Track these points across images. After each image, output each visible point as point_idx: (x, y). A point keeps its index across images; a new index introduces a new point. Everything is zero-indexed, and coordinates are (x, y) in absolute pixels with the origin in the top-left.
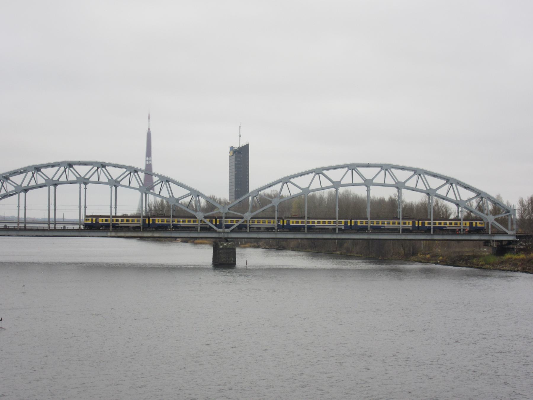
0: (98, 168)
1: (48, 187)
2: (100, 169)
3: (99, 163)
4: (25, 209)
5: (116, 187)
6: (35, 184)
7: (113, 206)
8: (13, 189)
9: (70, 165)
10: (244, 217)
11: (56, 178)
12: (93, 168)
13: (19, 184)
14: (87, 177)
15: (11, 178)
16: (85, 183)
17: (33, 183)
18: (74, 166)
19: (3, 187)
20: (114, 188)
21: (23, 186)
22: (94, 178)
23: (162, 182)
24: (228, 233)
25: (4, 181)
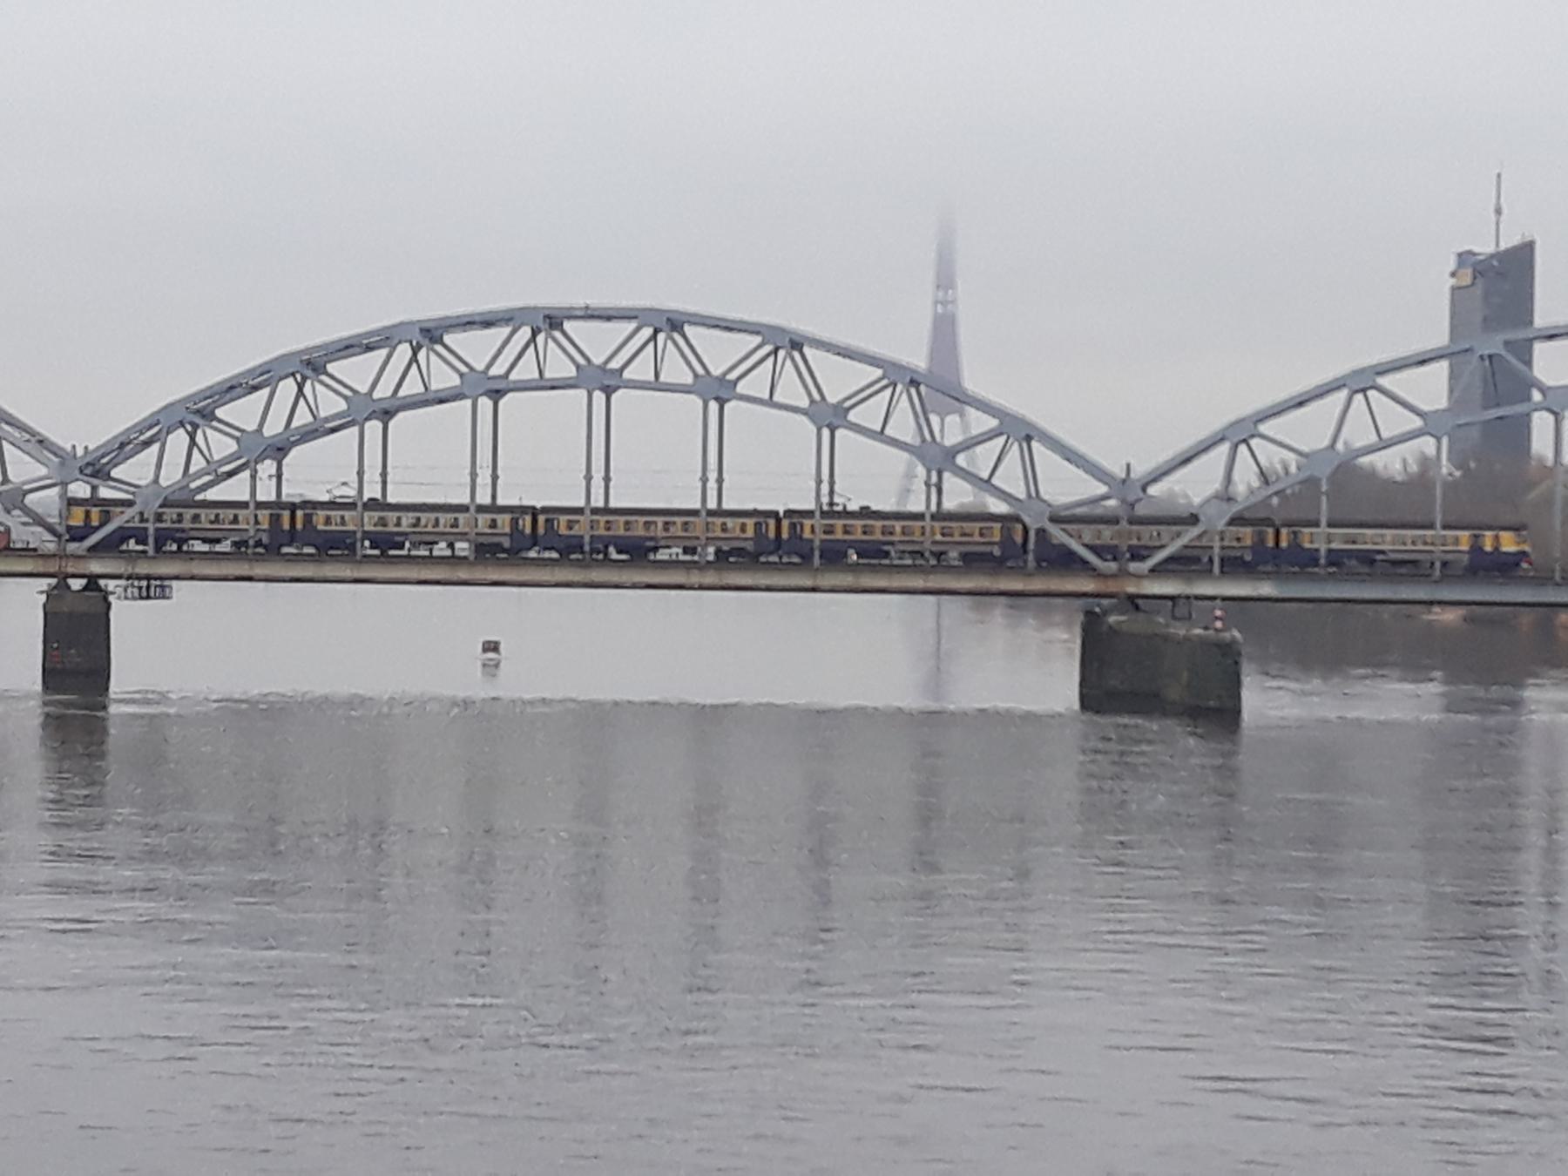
0: (656, 331)
1: (468, 403)
2: (661, 337)
4: (384, 483)
5: (722, 402)
6: (422, 389)
8: (342, 405)
9: (553, 321)
10: (1202, 518)
14: (615, 364)
15: (330, 368)
16: (608, 386)
17: (413, 386)
18: (567, 325)
19: (302, 399)
20: (713, 406)
21: (376, 395)
22: (641, 370)
23: (895, 386)
24: (1139, 577)
25: (304, 378)
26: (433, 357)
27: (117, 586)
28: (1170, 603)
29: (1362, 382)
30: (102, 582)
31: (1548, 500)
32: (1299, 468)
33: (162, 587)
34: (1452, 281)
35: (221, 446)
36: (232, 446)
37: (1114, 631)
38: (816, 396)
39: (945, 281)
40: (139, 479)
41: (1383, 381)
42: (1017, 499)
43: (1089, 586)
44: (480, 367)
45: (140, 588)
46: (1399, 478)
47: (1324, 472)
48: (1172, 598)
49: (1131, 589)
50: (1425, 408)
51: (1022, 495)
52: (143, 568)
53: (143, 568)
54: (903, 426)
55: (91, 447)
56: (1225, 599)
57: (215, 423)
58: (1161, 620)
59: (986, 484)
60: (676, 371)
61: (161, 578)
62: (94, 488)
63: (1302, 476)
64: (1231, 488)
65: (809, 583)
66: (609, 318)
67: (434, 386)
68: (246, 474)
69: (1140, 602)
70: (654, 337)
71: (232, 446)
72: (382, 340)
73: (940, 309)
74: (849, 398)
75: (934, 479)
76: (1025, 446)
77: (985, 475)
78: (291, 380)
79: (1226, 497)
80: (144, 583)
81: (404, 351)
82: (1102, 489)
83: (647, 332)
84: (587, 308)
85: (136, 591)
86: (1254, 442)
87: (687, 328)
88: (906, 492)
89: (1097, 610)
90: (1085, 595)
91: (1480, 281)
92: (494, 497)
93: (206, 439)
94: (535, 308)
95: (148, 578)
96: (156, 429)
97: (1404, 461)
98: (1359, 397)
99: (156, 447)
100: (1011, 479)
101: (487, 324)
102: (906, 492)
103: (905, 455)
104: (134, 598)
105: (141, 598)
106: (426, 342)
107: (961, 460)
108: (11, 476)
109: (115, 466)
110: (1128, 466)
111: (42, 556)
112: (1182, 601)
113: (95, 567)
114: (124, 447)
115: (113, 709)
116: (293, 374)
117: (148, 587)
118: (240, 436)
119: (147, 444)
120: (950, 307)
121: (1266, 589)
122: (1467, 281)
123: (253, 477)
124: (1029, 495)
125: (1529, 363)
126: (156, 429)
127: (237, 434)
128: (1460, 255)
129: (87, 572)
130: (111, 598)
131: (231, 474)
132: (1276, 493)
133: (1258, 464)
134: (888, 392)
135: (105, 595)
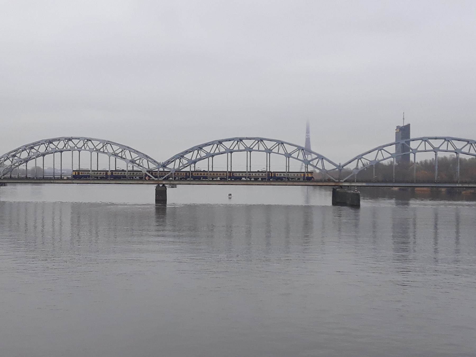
0: (258, 141)
1: (226, 154)
2: (259, 142)
3: (259, 138)
4: (212, 168)
6: (219, 152)
7: (268, 166)
8: (205, 155)
9: (241, 140)
11: (231, 148)
12: (255, 141)
13: (209, 152)
14: (251, 147)
15: (203, 148)
16: (250, 151)
17: (217, 151)
18: (243, 141)
20: (268, 154)
21: (211, 153)
23: (299, 150)
24: (342, 182)
25: (199, 150)
26: (220, 146)
27: (168, 186)
28: (347, 187)
29: (380, 149)
30: (165, 185)
31: (413, 168)
32: (370, 163)
33: (175, 186)
34: (396, 131)
35: (185, 162)
36: (187, 162)
37: (338, 191)
38: (286, 152)
39: (308, 132)
40: (172, 167)
41: (384, 148)
42: (321, 170)
43: (333, 184)
44: (228, 148)
45: (172, 186)
46: (387, 165)
47: (374, 164)
48: (348, 186)
49: (341, 184)
50: (391, 153)
51: (322, 169)
52: (172, 183)
53: (172, 183)
54: (301, 157)
55: (163, 162)
56: (357, 186)
57: (184, 158)
58: (346, 190)
59: (315, 167)
60: (262, 148)
61: (175, 184)
62: (164, 169)
63: (371, 164)
64: (358, 167)
65: (285, 184)
66: (250, 139)
67: (221, 151)
68: (189, 167)
69: (342, 187)
70: (258, 142)
71: (187, 162)
72: (212, 143)
73: (307, 137)
74: (292, 152)
75: (306, 166)
76: (322, 160)
77: (315, 165)
78: (196, 151)
79: (357, 168)
80: (172, 185)
81: (216, 145)
82: (335, 167)
83: (257, 141)
84: (247, 137)
85: (171, 186)
86: (362, 159)
87: (264, 141)
88: (302, 168)
89: (335, 188)
90: (332, 186)
91: (401, 131)
92: (231, 170)
93: (182, 161)
94: (238, 138)
95: (173, 184)
96: (174, 159)
97: (388, 162)
98: (380, 151)
99: (174, 162)
100: (320, 166)
101: (230, 140)
102: (302, 168)
103: (301, 162)
104: (170, 188)
105: (172, 188)
106: (219, 144)
107: (311, 163)
108: (150, 167)
109: (167, 165)
110: (340, 164)
111: (155, 181)
112: (350, 187)
113: (164, 182)
114: (169, 162)
115: (167, 206)
116: (197, 150)
117: (173, 186)
118: (188, 160)
119: (173, 161)
120: (309, 137)
121: (364, 184)
122: (398, 131)
123: (190, 167)
124: (323, 169)
125: (409, 145)
126: (173, 159)
127: (188, 160)
128: (397, 127)
129: (163, 183)
130: (167, 188)
131: (187, 166)
132: (366, 168)
133: (362, 162)
134: (298, 151)
135: (166, 187)
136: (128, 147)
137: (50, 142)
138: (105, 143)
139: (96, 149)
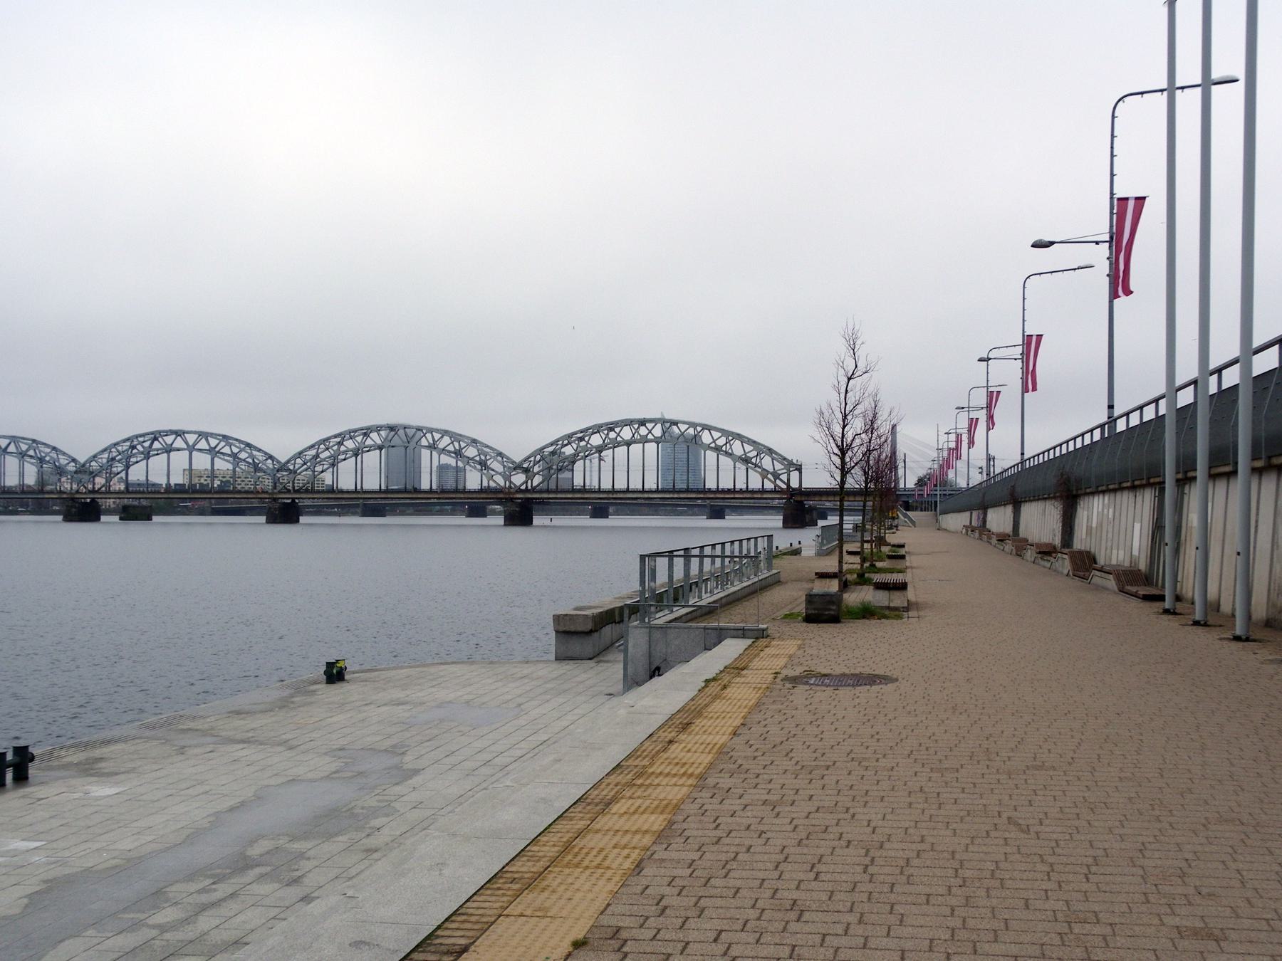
136: (739, 435)
137: (611, 427)
138: (636, 426)
139: (610, 439)
